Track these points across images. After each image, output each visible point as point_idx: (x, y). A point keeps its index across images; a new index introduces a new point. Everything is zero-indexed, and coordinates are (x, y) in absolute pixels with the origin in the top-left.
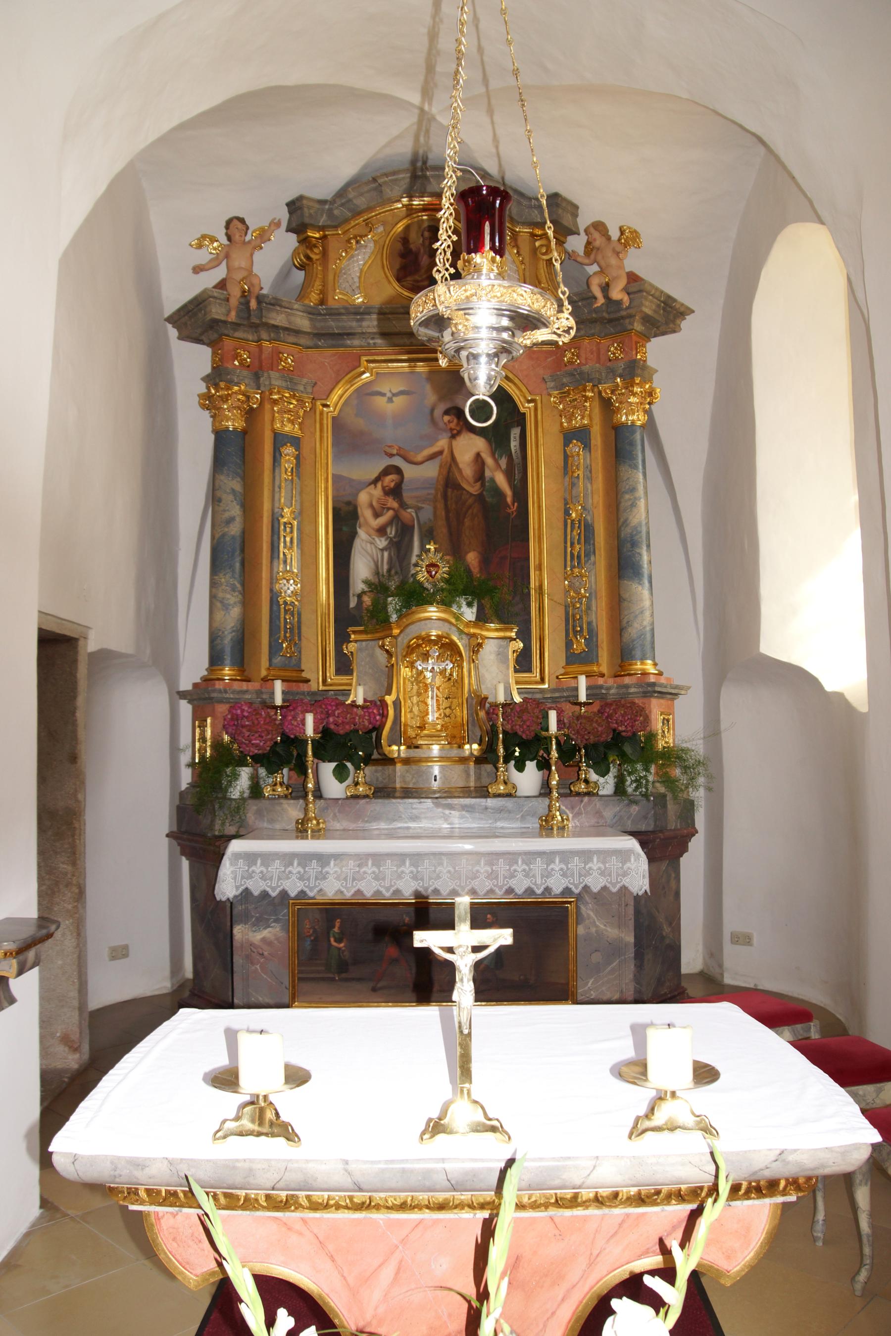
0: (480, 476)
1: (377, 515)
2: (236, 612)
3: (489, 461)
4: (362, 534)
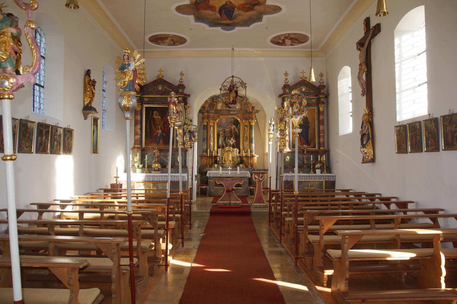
0: (234, 130)
1: (222, 135)
2: (206, 146)
3: (236, 128)
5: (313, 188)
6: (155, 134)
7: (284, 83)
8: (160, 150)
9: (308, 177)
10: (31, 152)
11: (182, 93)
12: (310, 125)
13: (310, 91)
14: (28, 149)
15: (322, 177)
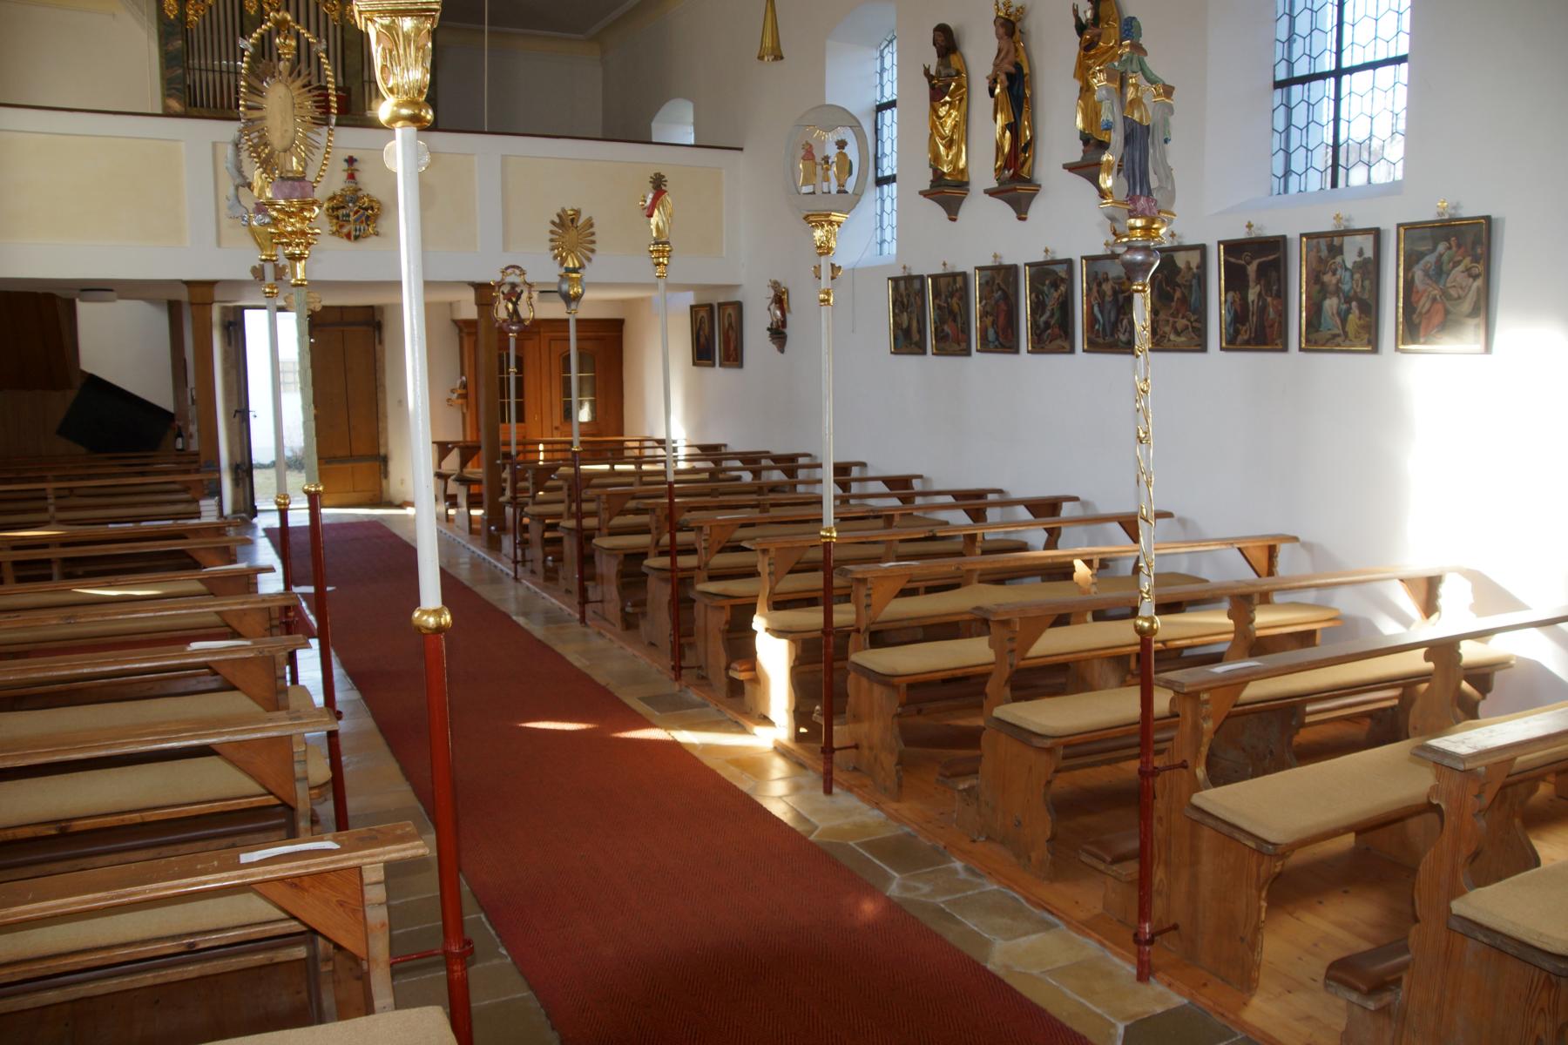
10: (1202, 347)
14: (1183, 339)
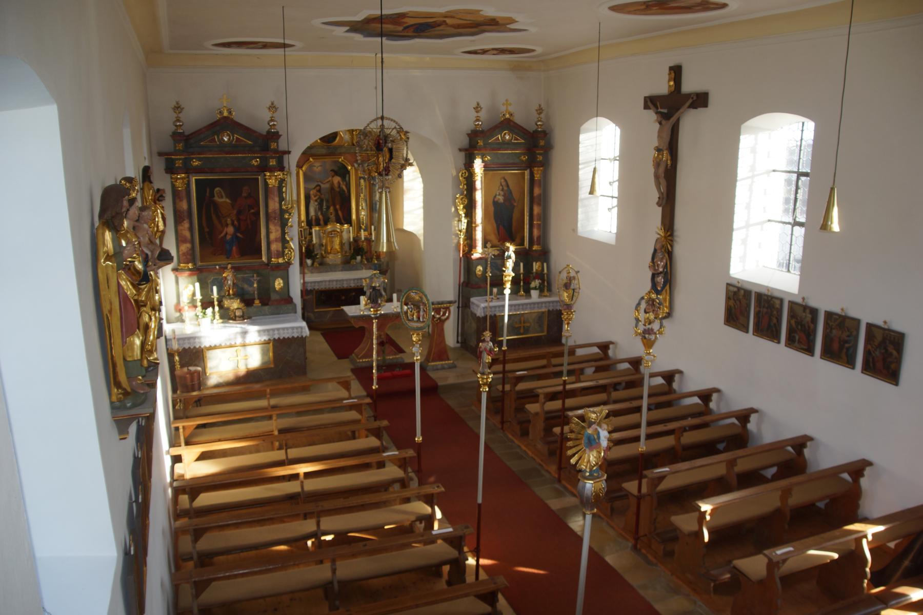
0: (339, 186)
1: (315, 196)
3: (341, 183)
4: (312, 202)
5: (528, 325)
6: (220, 237)
7: (472, 127)
8: (236, 269)
9: (521, 307)
11: (276, 151)
12: (515, 204)
13: (517, 140)
15: (544, 305)
